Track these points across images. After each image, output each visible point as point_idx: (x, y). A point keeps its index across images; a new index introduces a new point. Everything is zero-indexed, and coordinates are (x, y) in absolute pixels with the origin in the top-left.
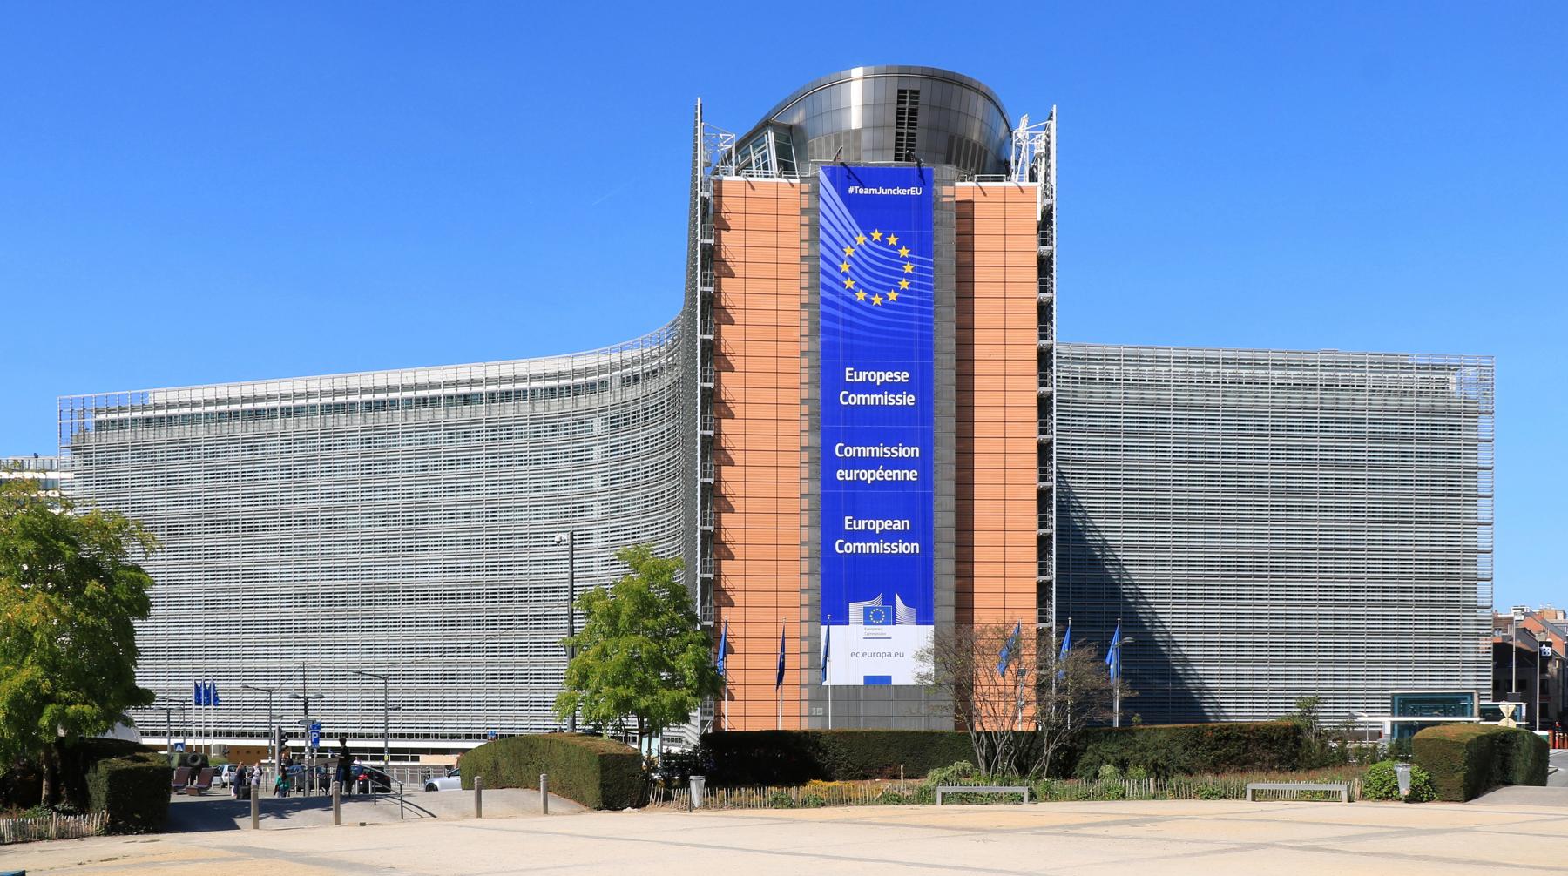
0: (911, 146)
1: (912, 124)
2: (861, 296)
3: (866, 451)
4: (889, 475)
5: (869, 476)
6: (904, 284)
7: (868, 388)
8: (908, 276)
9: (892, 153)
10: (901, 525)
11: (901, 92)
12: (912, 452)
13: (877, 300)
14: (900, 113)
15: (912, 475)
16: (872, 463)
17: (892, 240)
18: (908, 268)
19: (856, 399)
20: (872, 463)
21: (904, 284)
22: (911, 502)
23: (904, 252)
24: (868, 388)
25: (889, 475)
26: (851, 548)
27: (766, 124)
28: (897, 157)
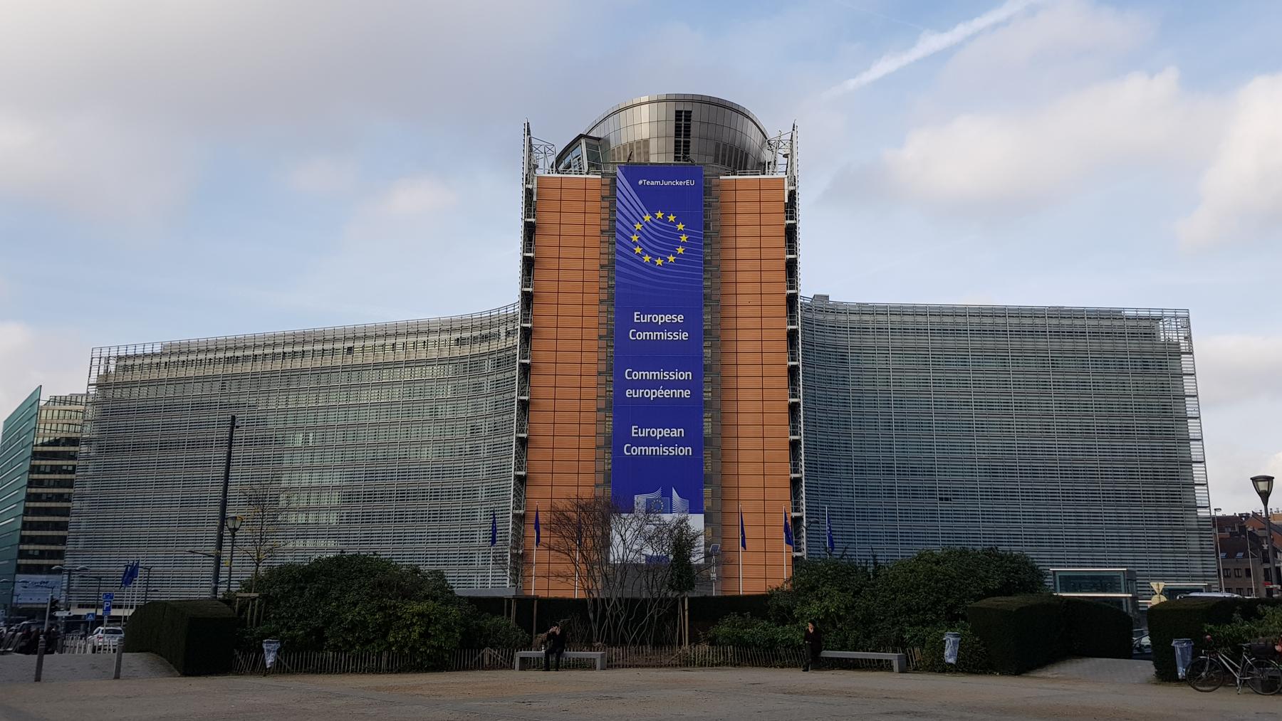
0: (687, 151)
1: (687, 135)
2: (647, 258)
3: (649, 375)
4: (667, 393)
5: (652, 394)
6: (680, 250)
7: (652, 327)
8: (683, 244)
9: (673, 156)
10: (676, 433)
11: (678, 113)
12: (686, 375)
13: (659, 262)
14: (678, 128)
15: (686, 394)
16: (654, 384)
17: (672, 218)
18: (684, 238)
19: (642, 336)
20: (654, 384)
21: (680, 250)
22: (684, 414)
23: (680, 227)
24: (652, 327)
25: (667, 393)
26: (637, 451)
27: (581, 136)
28: (676, 158)
